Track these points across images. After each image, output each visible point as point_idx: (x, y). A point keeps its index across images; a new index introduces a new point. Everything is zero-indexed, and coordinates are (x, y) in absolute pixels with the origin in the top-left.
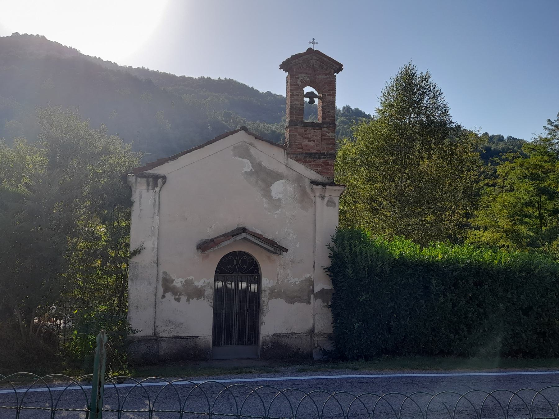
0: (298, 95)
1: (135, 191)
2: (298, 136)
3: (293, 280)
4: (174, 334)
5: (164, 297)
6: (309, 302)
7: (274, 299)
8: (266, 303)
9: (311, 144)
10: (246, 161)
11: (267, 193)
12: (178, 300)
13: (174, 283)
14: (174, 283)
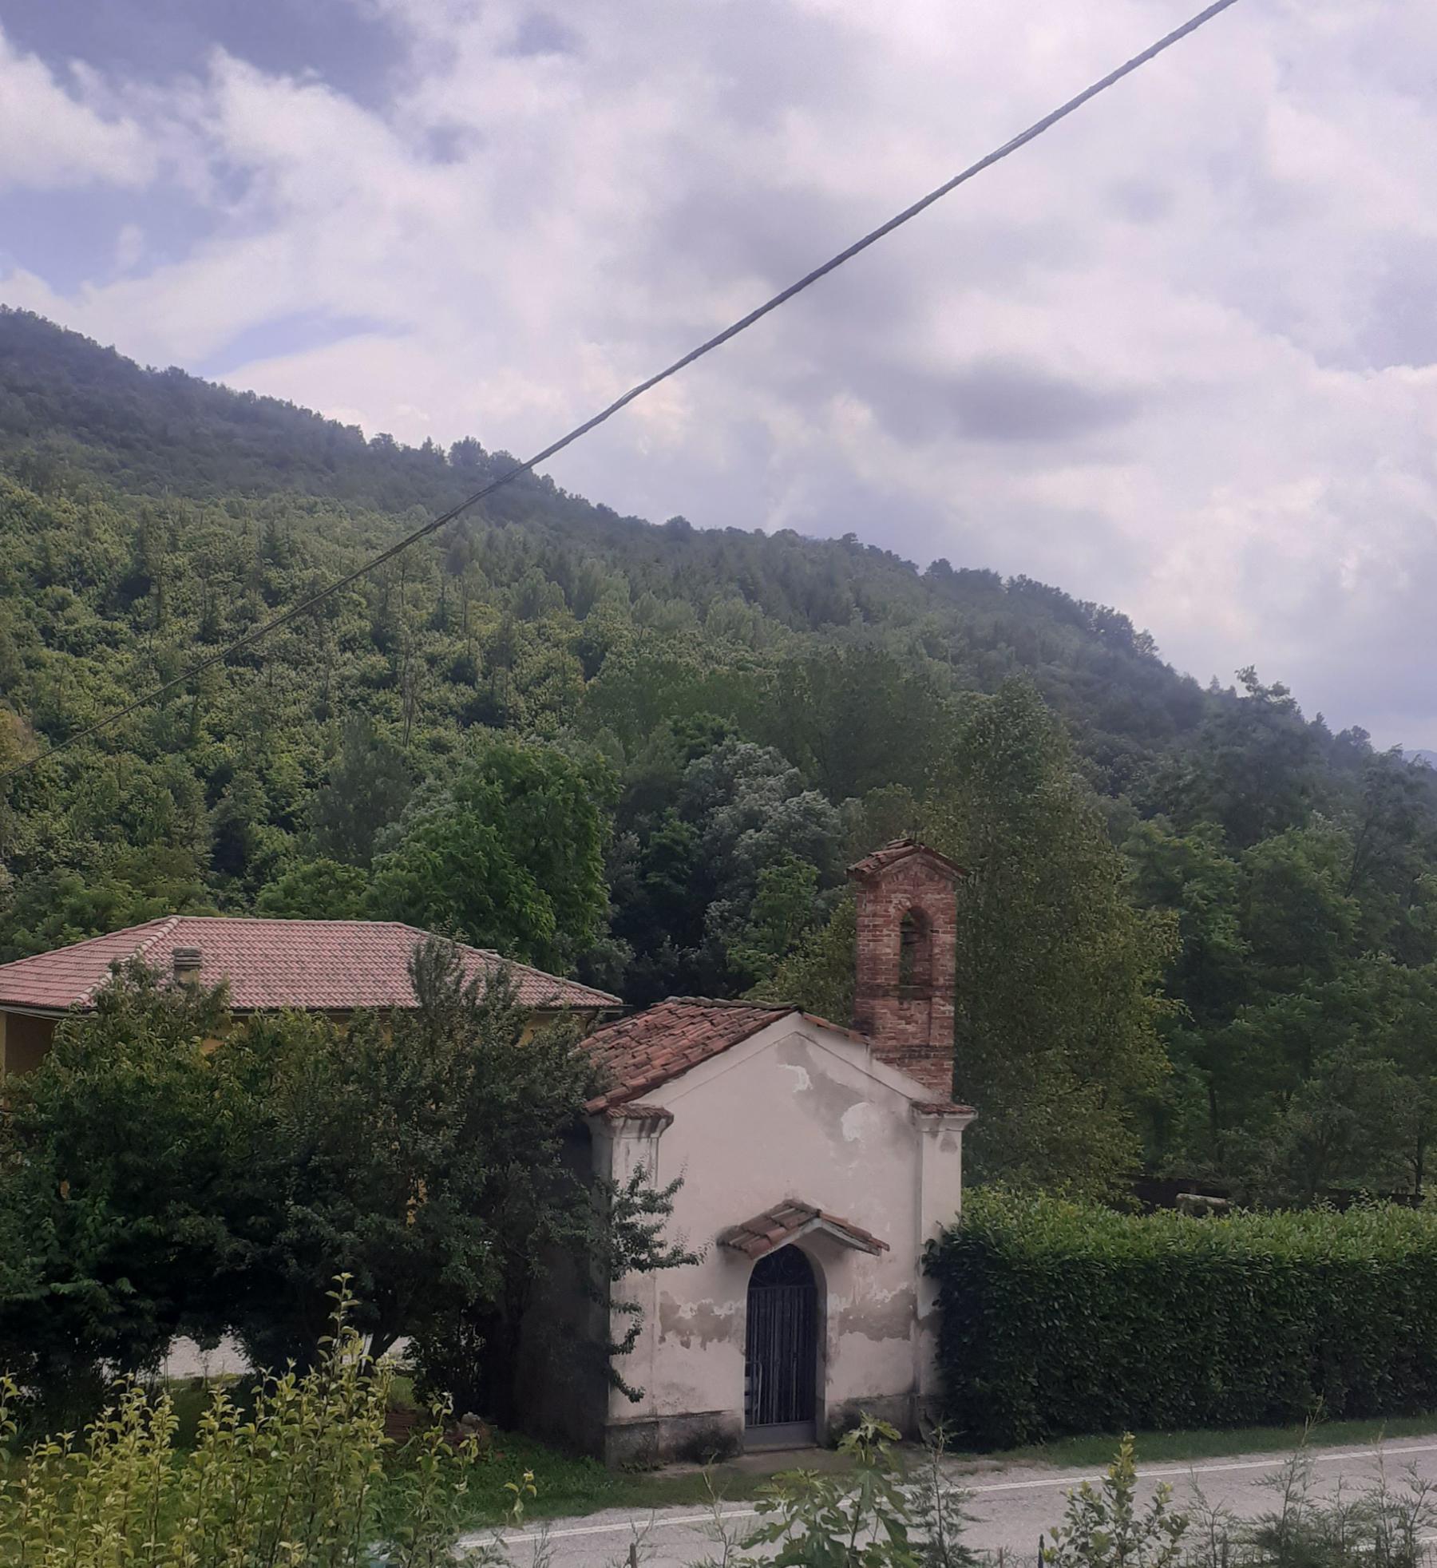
0: (889, 935)
1: (618, 1143)
2: (889, 1015)
3: (879, 1297)
4: (681, 1410)
5: (663, 1339)
6: (907, 1337)
7: (847, 1334)
8: (834, 1341)
9: (911, 1028)
10: (800, 1070)
11: (833, 1128)
12: (686, 1344)
13: (681, 1314)
14: (681, 1314)
